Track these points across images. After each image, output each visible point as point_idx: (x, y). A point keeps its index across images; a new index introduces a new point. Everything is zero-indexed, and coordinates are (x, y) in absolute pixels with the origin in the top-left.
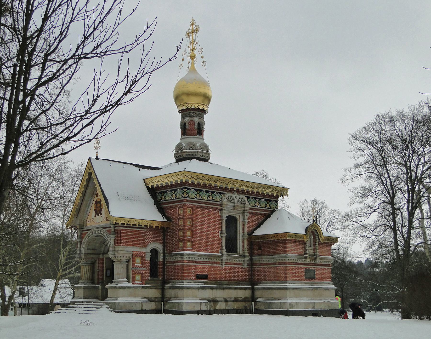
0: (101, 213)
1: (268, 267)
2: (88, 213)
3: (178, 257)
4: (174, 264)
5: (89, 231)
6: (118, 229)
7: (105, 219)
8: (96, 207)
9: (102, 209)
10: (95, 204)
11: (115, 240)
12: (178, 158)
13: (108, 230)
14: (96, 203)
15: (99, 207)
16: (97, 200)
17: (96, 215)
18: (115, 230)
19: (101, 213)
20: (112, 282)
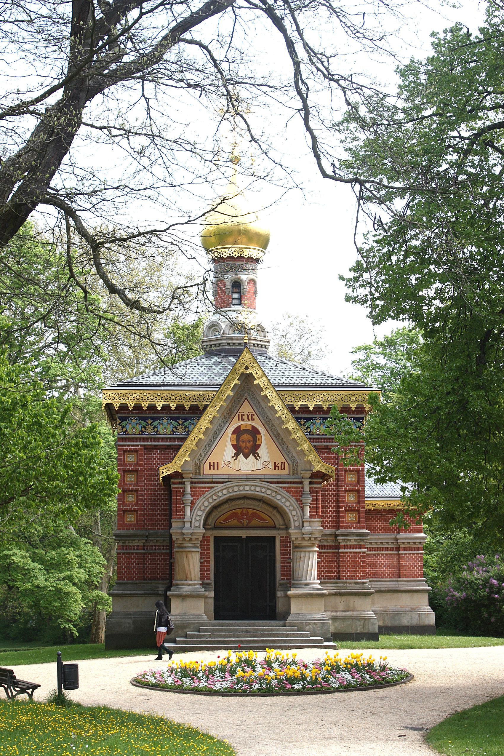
0: (258, 454)
1: (378, 554)
2: (212, 449)
3: (350, 538)
4: (340, 551)
5: (220, 485)
6: (315, 488)
7: (271, 466)
8: (238, 439)
9: (260, 445)
10: (233, 433)
11: (310, 507)
12: (233, 347)
13: (284, 488)
14: (237, 431)
15: (249, 441)
16: (239, 426)
17: (236, 456)
18: (310, 488)
19: (256, 456)
20: (296, 586)
